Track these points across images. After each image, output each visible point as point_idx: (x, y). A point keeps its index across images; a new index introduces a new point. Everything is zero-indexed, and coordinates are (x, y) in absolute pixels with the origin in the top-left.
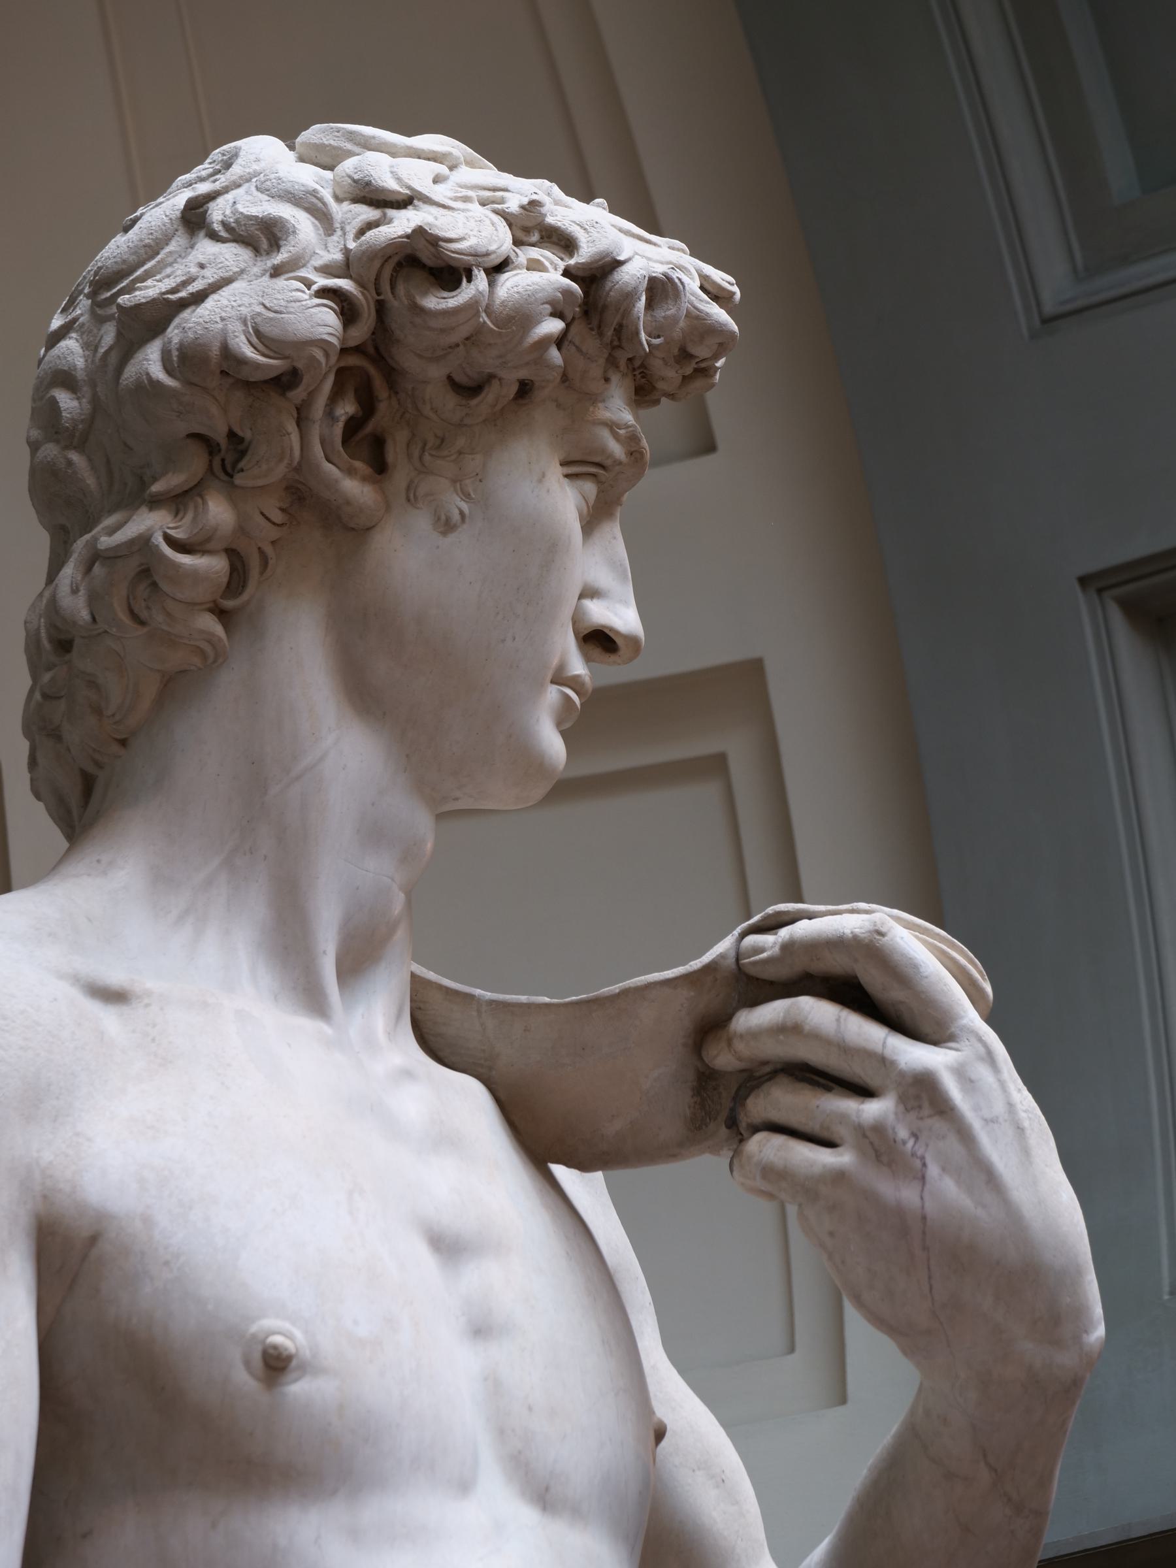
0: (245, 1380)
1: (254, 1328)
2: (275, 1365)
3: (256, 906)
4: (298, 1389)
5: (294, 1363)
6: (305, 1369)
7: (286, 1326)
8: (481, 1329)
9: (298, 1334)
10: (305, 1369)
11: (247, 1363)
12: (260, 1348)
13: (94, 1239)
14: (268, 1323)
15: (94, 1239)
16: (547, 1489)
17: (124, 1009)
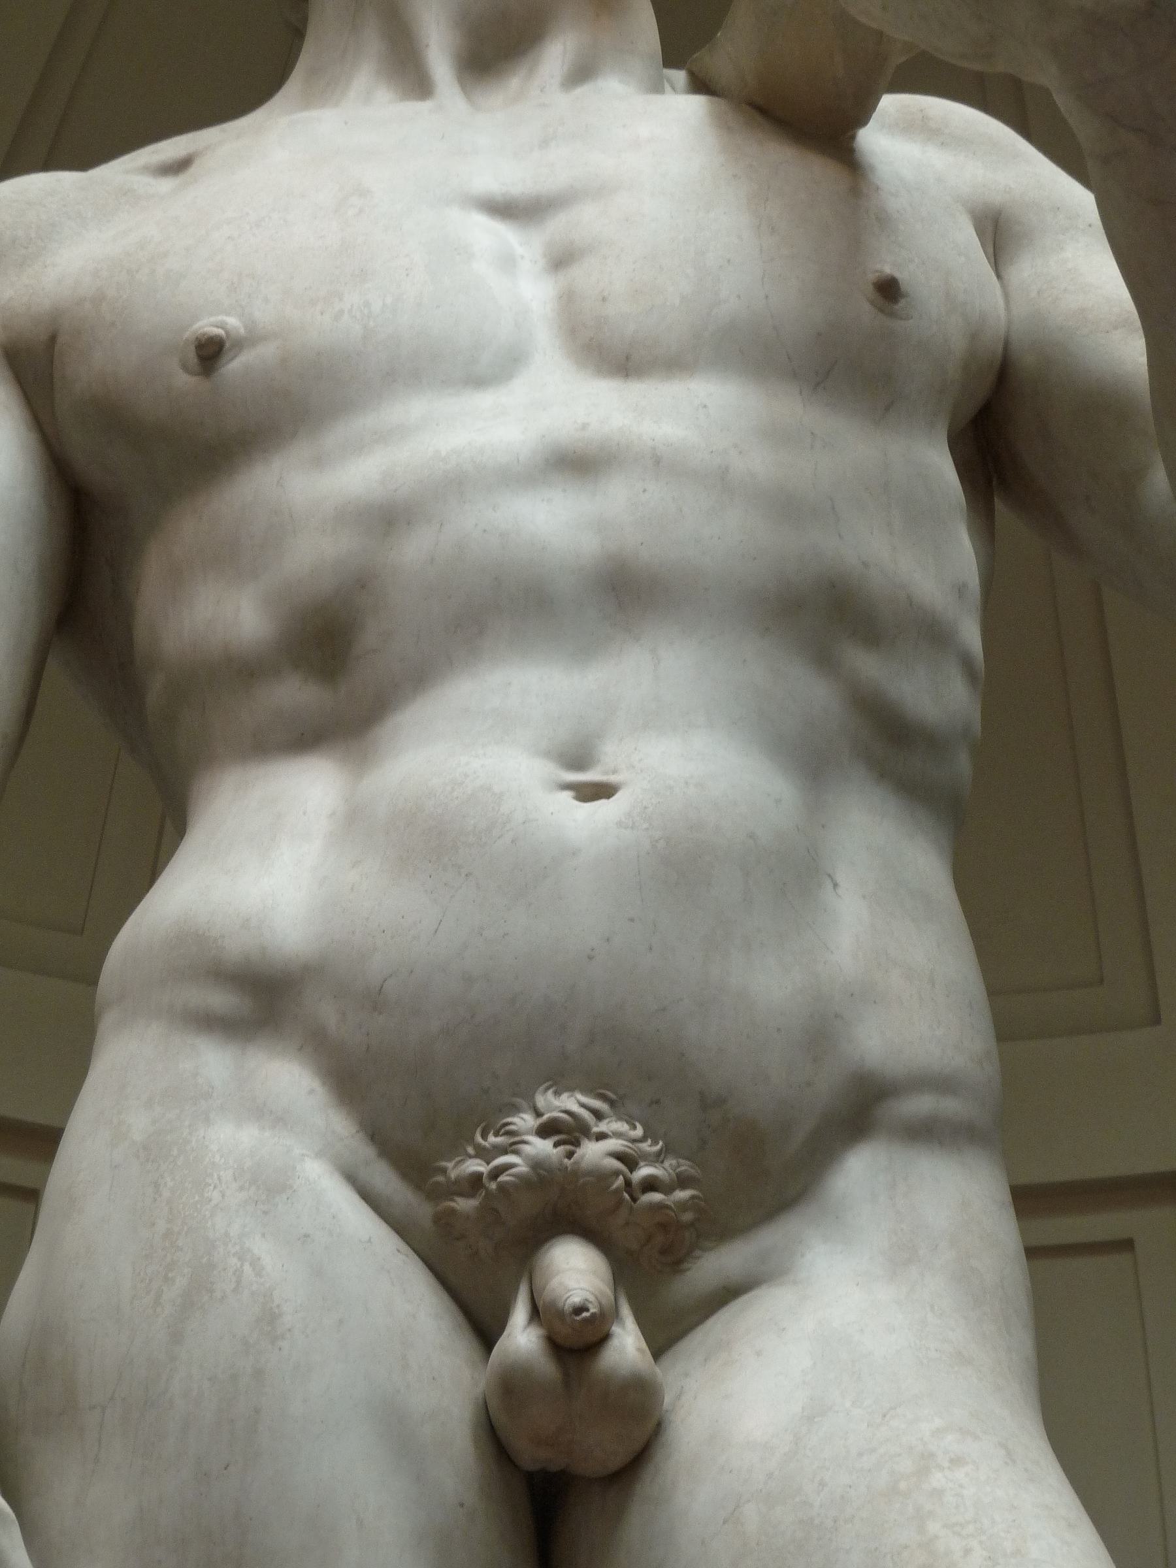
0: (184, 381)
1: (187, 335)
2: (210, 353)
3: (373, 43)
4: (233, 366)
5: (227, 345)
6: (240, 344)
7: (220, 318)
8: (560, 260)
9: (233, 322)
10: (240, 344)
11: (185, 368)
12: (193, 348)
13: (53, 339)
14: (196, 326)
15: (53, 339)
16: (627, 358)
17: (192, 170)
